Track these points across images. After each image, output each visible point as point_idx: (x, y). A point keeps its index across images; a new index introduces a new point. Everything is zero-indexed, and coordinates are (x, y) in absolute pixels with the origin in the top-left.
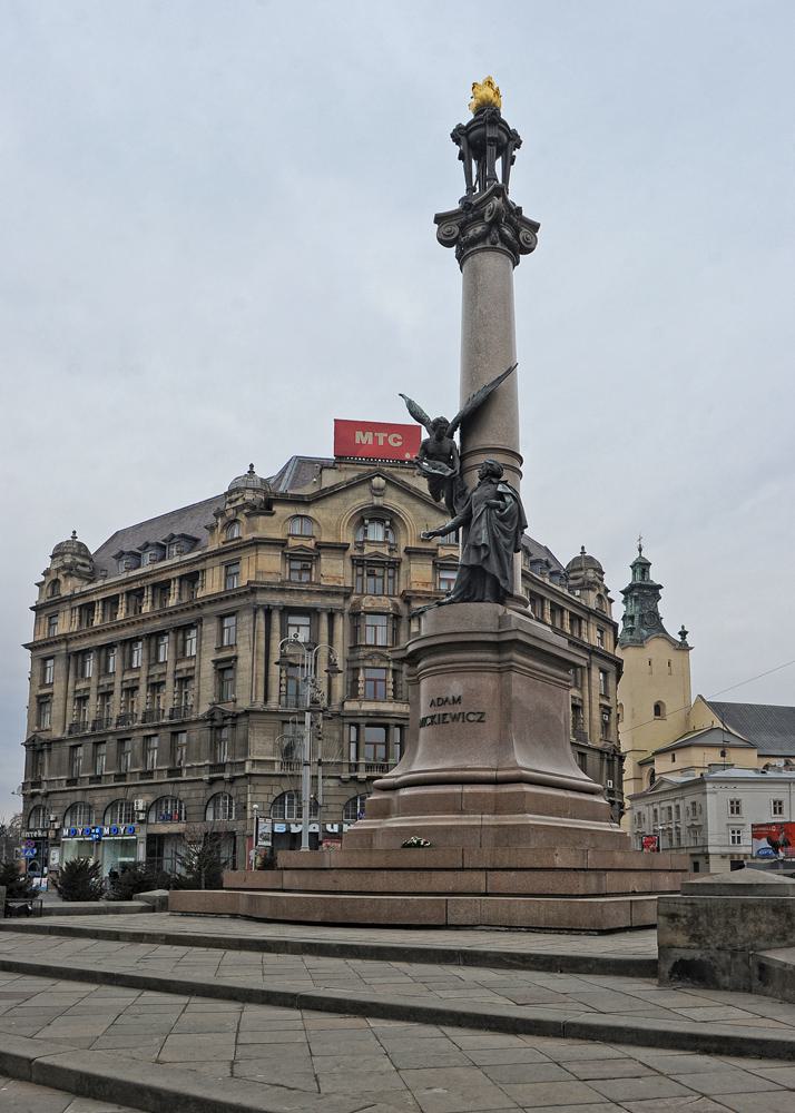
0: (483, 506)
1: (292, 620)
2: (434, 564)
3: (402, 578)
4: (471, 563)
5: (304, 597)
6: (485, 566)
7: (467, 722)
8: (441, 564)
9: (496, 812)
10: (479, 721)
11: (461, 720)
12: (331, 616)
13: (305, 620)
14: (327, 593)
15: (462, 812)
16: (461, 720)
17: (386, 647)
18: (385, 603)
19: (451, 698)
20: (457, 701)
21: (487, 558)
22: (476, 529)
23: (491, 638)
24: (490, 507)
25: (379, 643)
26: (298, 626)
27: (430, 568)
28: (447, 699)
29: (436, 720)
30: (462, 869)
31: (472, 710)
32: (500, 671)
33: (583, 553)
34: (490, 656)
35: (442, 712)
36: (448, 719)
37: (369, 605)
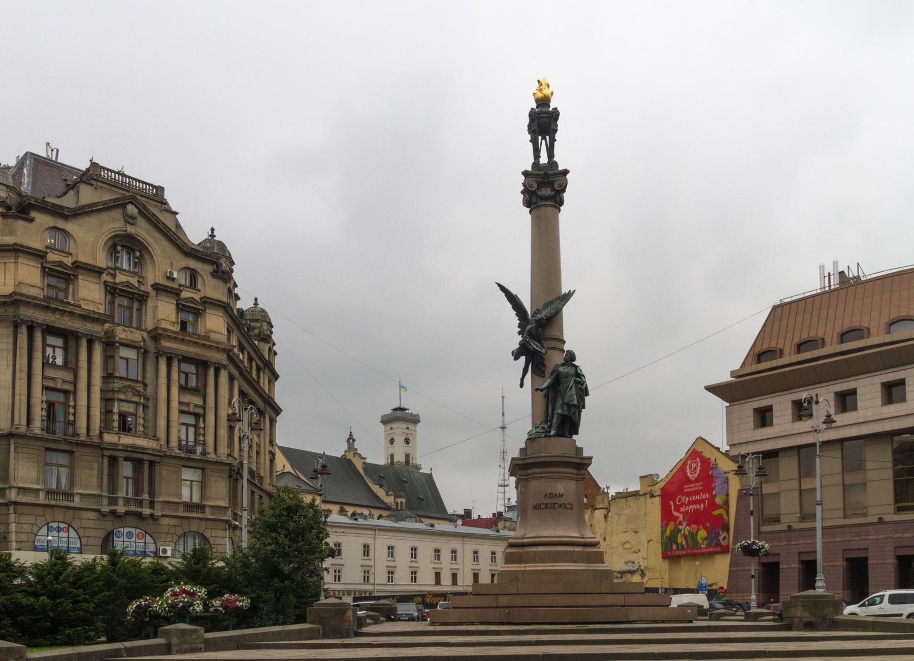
0: (572, 382)
1: (51, 340)
2: (178, 305)
3: (150, 313)
4: (566, 413)
5: (66, 319)
6: (572, 416)
8: (183, 305)
12: (90, 343)
13: (59, 342)
14: (87, 317)
17: (137, 381)
18: (136, 336)
22: (569, 393)
24: (576, 382)
25: (132, 376)
26: (54, 347)
27: (174, 307)
33: (256, 304)
34: (575, 471)
35: (554, 502)
37: (123, 336)
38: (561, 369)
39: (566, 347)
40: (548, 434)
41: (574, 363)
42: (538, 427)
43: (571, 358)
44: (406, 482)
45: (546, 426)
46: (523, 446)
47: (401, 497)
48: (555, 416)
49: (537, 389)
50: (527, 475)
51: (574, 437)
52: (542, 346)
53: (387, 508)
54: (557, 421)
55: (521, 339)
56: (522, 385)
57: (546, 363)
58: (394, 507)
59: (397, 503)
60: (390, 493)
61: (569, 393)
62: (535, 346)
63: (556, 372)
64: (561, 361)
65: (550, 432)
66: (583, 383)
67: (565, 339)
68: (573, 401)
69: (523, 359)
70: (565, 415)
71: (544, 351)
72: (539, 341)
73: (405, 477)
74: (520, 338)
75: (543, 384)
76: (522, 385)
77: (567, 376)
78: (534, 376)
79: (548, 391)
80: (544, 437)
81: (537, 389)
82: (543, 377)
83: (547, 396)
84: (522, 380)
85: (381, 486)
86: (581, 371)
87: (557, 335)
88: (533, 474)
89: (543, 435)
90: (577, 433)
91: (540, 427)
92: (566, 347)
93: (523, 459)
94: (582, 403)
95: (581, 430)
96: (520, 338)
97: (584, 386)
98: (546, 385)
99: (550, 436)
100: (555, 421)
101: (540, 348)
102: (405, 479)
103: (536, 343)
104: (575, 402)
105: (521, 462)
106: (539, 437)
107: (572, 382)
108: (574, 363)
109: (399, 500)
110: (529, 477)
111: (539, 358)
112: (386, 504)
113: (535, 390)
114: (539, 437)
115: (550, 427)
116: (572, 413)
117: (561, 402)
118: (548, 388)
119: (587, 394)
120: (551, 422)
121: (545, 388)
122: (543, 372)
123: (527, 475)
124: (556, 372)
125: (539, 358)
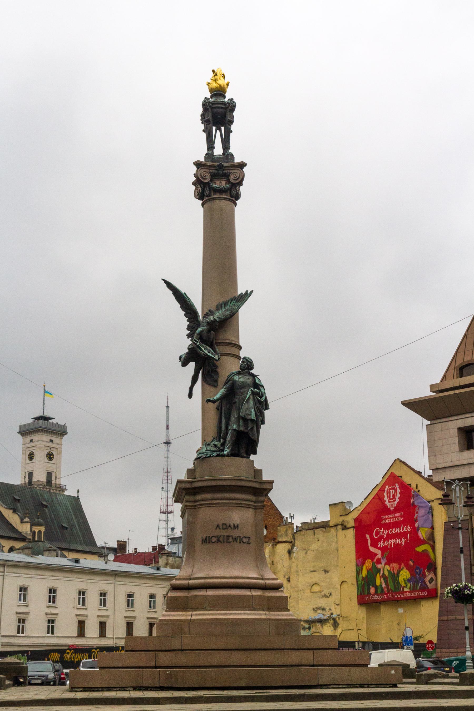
4: (242, 429)
6: (250, 433)
7: (242, 542)
9: (269, 609)
10: (248, 543)
11: (238, 541)
15: (254, 609)
16: (238, 541)
19: (232, 525)
20: (236, 527)
21: (252, 428)
23: (257, 485)
24: (253, 393)
28: (230, 526)
29: (221, 539)
30: (284, 649)
31: (245, 535)
32: (256, 508)
35: (226, 534)
36: (231, 539)
38: (237, 378)
39: (242, 354)
40: (221, 453)
41: (251, 371)
42: (209, 445)
43: (248, 365)
44: (46, 506)
45: (218, 444)
46: (191, 466)
47: (39, 524)
48: (230, 432)
49: (209, 401)
50: (195, 502)
51: (252, 457)
52: (215, 352)
53: (22, 538)
54: (231, 438)
55: (191, 342)
56: (190, 395)
57: (219, 370)
58: (30, 537)
59: (34, 532)
60: (26, 519)
61: (245, 406)
62: (206, 352)
63: (231, 381)
64: (236, 369)
65: (223, 451)
66: (262, 395)
67: (241, 344)
68: (251, 415)
69: (192, 365)
70: (241, 431)
71: (216, 357)
72: (211, 346)
73: (45, 500)
74: (189, 342)
75: (215, 395)
76: (190, 395)
77: (243, 386)
78: (205, 385)
79: (221, 402)
80: (217, 456)
81: (209, 401)
82: (216, 386)
83: (219, 409)
84: (191, 389)
85: (15, 511)
86: (260, 380)
87: (233, 340)
88: (203, 500)
89: (215, 454)
90: (255, 453)
91: (212, 444)
92: (242, 354)
93: (191, 482)
94: (261, 418)
95: (259, 449)
96: (189, 342)
97: (264, 398)
98: (218, 396)
99: (223, 456)
100: (228, 438)
101: (212, 354)
102: (45, 503)
103: (208, 348)
104: (253, 417)
105: (188, 486)
106: (210, 457)
107: (249, 394)
108: (251, 371)
109: (36, 529)
110: (196, 504)
111: (211, 365)
112: (20, 533)
113: (207, 401)
114: (210, 457)
115: (223, 444)
116: (249, 429)
117: (236, 416)
118: (221, 399)
119: (267, 408)
120: (225, 439)
121: (218, 400)
122: (216, 381)
123: (195, 502)
124: (231, 381)
125: (211, 365)
